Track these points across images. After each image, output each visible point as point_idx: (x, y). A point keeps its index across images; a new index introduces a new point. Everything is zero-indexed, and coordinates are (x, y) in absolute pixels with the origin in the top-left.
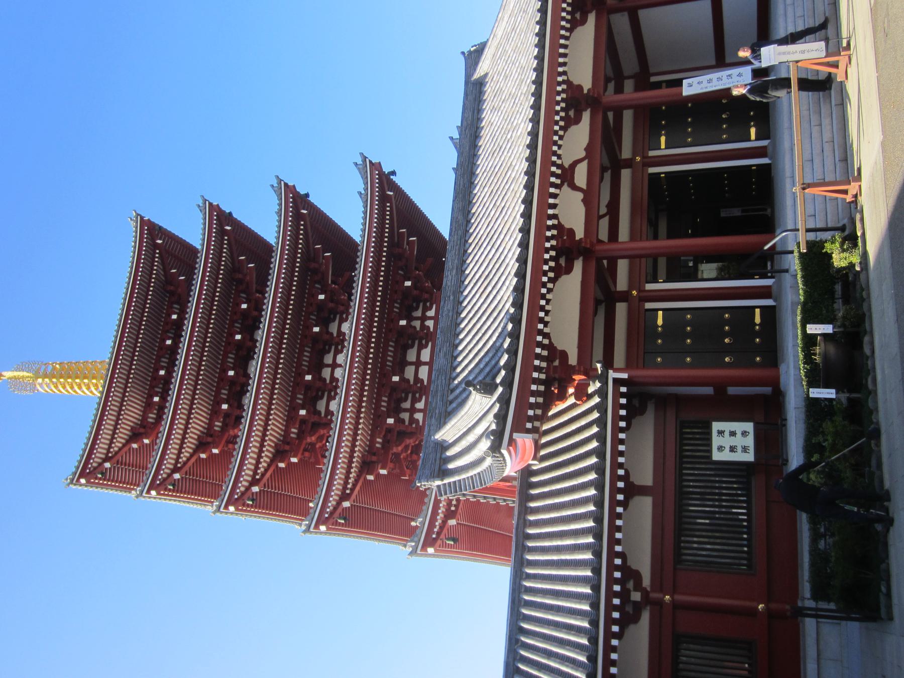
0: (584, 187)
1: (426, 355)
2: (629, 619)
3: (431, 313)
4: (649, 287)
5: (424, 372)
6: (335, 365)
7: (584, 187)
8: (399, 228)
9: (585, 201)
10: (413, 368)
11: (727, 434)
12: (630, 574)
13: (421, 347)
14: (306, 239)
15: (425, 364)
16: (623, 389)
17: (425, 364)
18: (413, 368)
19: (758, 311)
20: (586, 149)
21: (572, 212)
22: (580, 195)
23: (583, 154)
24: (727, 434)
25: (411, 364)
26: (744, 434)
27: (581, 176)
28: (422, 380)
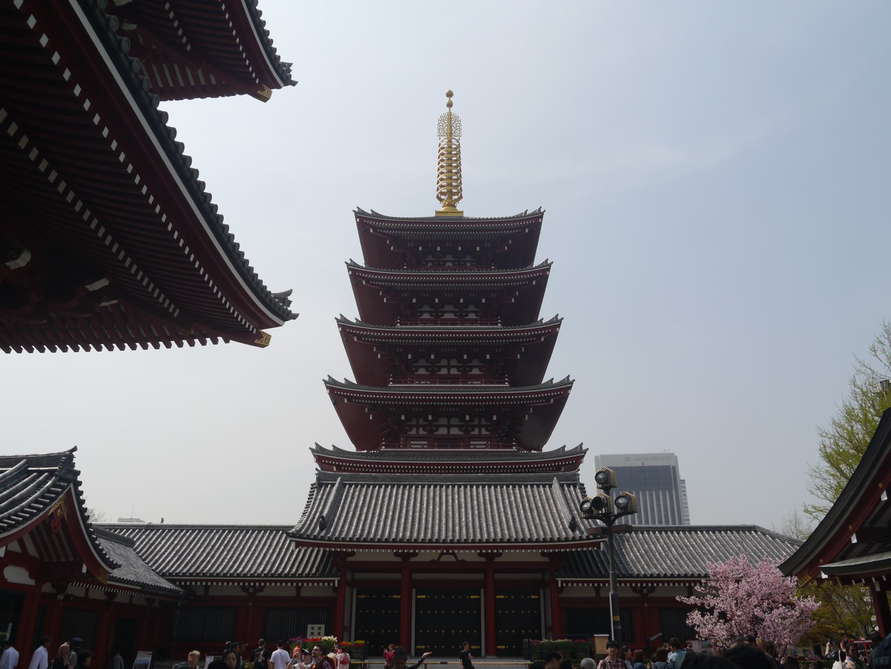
1: (455, 431)
2: (244, 588)
3: (484, 432)
4: (414, 591)
5: (443, 431)
6: (449, 367)
8: (533, 408)
9: (433, 561)
12: (261, 589)
13: (460, 427)
14: (526, 342)
15: (449, 431)
17: (449, 431)
19: (418, 647)
21: (425, 556)
22: (436, 558)
23: (460, 558)
25: (449, 422)
27: (445, 559)
28: (437, 430)
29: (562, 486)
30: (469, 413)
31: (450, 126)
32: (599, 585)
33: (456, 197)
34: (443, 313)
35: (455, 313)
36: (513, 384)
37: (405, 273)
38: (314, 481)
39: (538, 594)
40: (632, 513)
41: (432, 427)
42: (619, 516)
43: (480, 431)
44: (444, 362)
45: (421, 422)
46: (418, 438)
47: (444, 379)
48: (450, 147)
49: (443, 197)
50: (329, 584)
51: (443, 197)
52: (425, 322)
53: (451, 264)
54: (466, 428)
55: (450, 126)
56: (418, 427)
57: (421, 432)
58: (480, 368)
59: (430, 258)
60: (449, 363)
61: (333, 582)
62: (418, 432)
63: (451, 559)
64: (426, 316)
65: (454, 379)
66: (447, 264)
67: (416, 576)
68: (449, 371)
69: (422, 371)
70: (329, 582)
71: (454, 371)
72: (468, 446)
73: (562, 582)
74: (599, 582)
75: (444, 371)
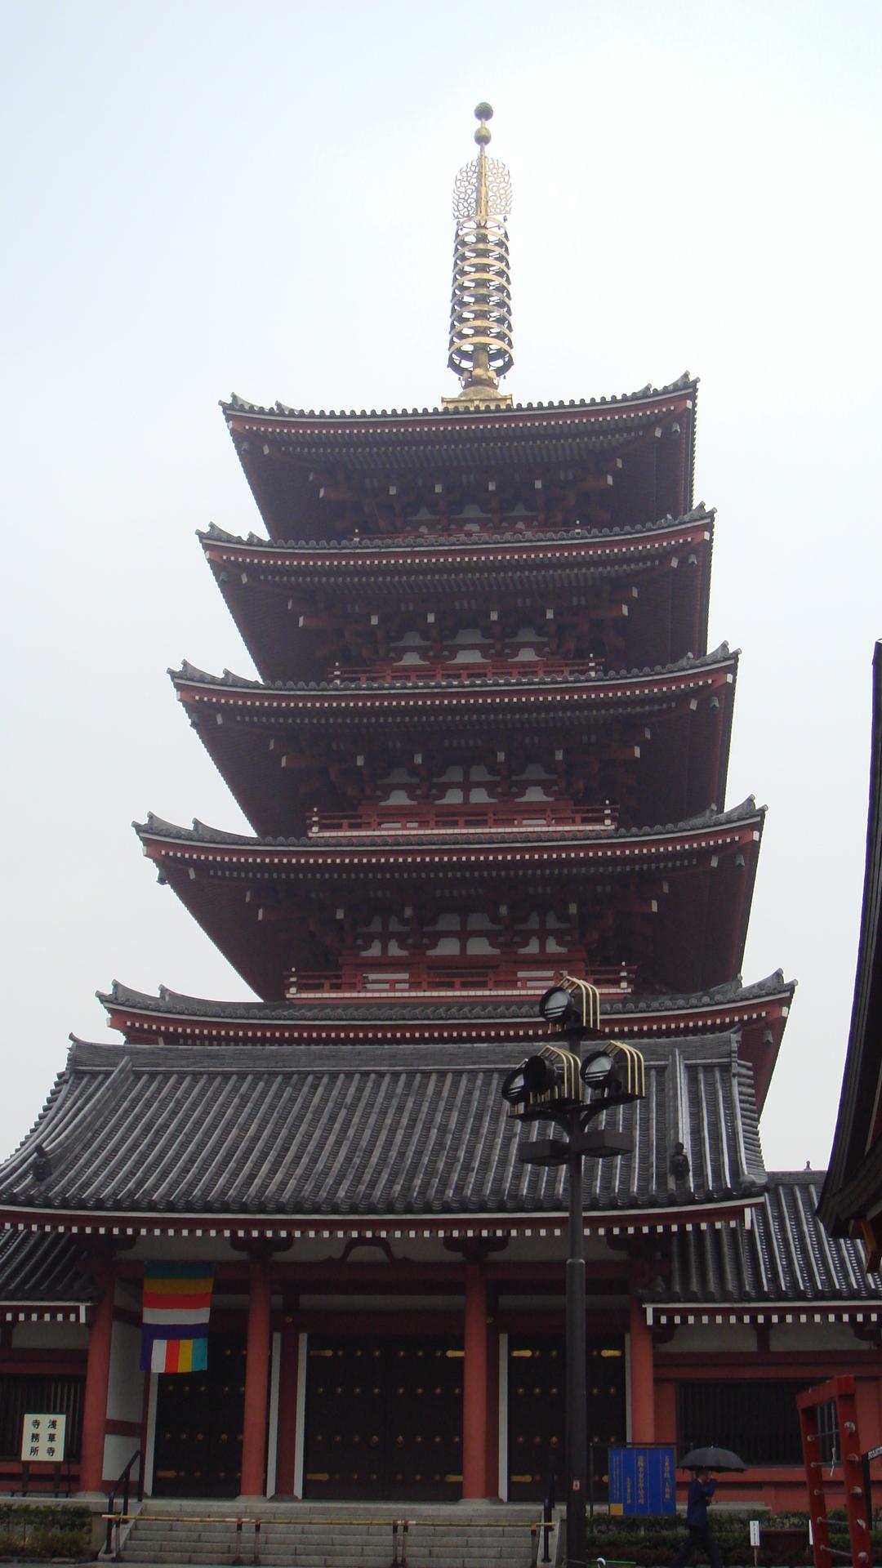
0: (349, 1259)
1: (479, 947)
3: (552, 947)
4: (303, 1339)
5: (448, 948)
6: (466, 787)
7: (349, 1259)
9: (330, 1262)
10: (457, 927)
11: (52, 1431)
13: (491, 937)
15: (463, 948)
16: (73, 1317)
17: (463, 948)
18: (457, 927)
20: (406, 1262)
22: (337, 1254)
23: (398, 1253)
24: (52, 1431)
25: (464, 924)
26: (51, 1451)
27: (360, 1254)
28: (434, 946)
29: (692, 1070)
30: (516, 903)
31: (479, 189)
32: (768, 1319)
33: (499, 363)
34: (454, 651)
35: (484, 650)
36: (620, 822)
37: (358, 552)
38: (62, 1066)
39: (621, 1347)
40: (629, 1099)
41: (420, 936)
42: (598, 1106)
43: (543, 946)
44: (455, 774)
45: (394, 926)
46: (385, 964)
47: (448, 817)
48: (482, 239)
49: (466, 364)
50: (66, 1317)
51: (466, 364)
52: (405, 673)
53: (475, 527)
54: (508, 937)
55: (479, 189)
56: (385, 937)
57: (395, 950)
58: (546, 787)
59: (424, 514)
60: (467, 774)
61: (76, 1310)
62: (385, 949)
63: (378, 1254)
64: (411, 659)
65: (476, 816)
66: (468, 527)
67: (308, 1301)
68: (466, 797)
69: (399, 799)
70: (67, 1311)
71: (479, 797)
72: (512, 984)
73: (657, 1313)
74: (767, 1313)
75: (454, 797)
